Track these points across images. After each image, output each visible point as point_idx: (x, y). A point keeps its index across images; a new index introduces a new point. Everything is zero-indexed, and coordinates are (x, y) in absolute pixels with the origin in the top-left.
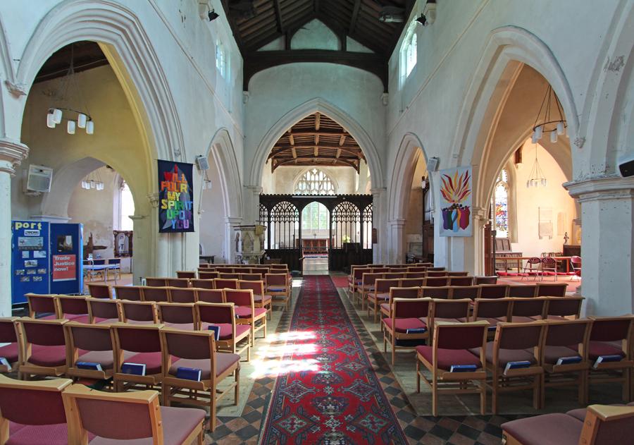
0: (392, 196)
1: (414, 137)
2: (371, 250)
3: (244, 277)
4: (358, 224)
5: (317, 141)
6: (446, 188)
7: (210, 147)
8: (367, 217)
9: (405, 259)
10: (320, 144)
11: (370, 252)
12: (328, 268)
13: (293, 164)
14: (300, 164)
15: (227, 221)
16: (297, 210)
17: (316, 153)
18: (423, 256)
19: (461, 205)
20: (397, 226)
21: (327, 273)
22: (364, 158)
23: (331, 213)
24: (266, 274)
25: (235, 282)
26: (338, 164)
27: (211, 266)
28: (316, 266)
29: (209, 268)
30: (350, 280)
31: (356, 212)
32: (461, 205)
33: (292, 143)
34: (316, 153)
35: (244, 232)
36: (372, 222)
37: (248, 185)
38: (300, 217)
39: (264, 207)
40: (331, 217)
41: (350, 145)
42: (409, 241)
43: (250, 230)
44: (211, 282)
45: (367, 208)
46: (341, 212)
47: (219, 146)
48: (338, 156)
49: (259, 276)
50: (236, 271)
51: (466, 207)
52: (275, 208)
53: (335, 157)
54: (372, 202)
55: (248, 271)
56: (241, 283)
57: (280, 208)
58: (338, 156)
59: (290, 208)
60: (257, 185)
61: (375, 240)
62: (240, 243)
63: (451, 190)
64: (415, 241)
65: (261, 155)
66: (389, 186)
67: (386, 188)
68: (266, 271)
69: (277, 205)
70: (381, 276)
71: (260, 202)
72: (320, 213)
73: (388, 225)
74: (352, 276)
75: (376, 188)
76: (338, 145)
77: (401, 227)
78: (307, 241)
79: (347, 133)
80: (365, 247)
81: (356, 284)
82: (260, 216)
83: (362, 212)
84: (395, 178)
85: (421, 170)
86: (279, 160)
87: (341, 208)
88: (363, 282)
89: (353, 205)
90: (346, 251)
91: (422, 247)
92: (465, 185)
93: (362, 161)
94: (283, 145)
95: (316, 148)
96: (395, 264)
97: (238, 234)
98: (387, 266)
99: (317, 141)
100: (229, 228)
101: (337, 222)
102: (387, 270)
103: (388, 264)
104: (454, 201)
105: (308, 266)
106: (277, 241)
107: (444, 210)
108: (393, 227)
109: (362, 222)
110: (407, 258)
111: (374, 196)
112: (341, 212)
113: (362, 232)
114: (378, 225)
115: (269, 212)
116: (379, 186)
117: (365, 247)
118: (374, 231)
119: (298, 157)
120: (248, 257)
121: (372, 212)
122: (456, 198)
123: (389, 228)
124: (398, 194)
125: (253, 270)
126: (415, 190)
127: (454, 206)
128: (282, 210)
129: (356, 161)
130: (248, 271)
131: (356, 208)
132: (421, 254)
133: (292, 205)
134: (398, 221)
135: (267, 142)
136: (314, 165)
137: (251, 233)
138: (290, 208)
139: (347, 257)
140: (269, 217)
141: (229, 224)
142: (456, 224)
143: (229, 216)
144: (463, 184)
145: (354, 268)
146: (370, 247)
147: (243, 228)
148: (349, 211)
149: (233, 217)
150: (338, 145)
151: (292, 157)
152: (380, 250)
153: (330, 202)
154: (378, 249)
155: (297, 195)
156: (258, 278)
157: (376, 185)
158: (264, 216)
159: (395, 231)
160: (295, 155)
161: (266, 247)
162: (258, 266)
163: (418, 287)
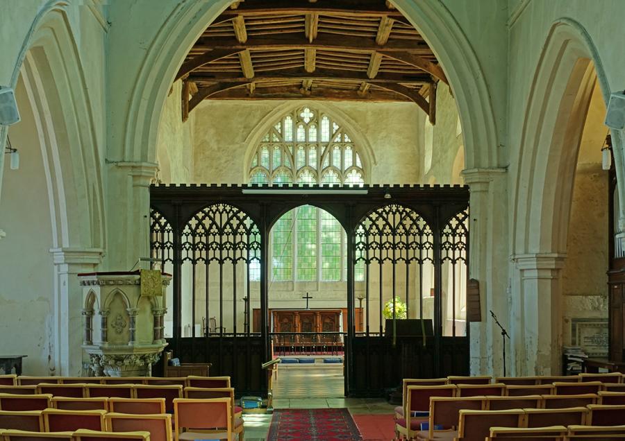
0: (523, 191)
1: (578, 32)
2: (465, 341)
3: (117, 407)
4: (428, 268)
5: (312, 31)
7: (18, 64)
9: (559, 363)
10: (321, 39)
11: (461, 345)
12: (342, 391)
13: (245, 95)
14: (262, 93)
15: (60, 258)
16: (255, 229)
17: (310, 67)
18: (610, 356)
20: (535, 274)
23: (351, 235)
24: (176, 400)
25: (98, 417)
26: (372, 95)
27: (24, 382)
28: (308, 383)
29: (15, 386)
30: (399, 416)
31: (421, 233)
33: (242, 36)
34: (310, 67)
35: (110, 290)
36: (467, 262)
37: (117, 158)
38: (263, 246)
39: (163, 221)
40: (352, 247)
41: (408, 44)
42: (570, 315)
43: (125, 284)
44: (37, 417)
45: (454, 222)
46: (381, 233)
47: (39, 52)
48: (372, 74)
49: (159, 404)
50: (94, 392)
52: (193, 222)
53: (363, 75)
54: (467, 205)
55: (125, 393)
56: (114, 420)
57: (207, 222)
58: (372, 74)
59: (235, 222)
60: (144, 157)
61: (474, 313)
62: (97, 320)
64: (587, 315)
65: (154, 73)
67: (506, 168)
68: (175, 393)
69: (200, 215)
70: (478, 404)
71: (152, 206)
72: (323, 235)
73: (513, 271)
74: (404, 410)
75: (477, 166)
76: (372, 42)
77: (549, 274)
79: (395, 10)
80: (447, 333)
81: (415, 428)
82: (152, 245)
83: (437, 233)
84: (530, 143)
85: (596, 126)
86: (202, 82)
87: (381, 223)
88: (430, 420)
89: (415, 215)
91: (606, 331)
93: (442, 87)
94: (216, 43)
95: (311, 52)
96: (532, 375)
97: (92, 295)
98: (500, 381)
99: (312, 31)
100: (65, 278)
102: (497, 391)
103: (501, 377)
105: (286, 385)
106: (201, 314)
108: (526, 274)
109: (438, 262)
110: (565, 361)
111: (471, 190)
112: (381, 233)
114: (483, 269)
115: (178, 233)
116: (485, 162)
117: (447, 333)
118: (473, 286)
119: (258, 75)
120: (119, 359)
121: (467, 234)
123: (516, 280)
124: (539, 186)
125: (139, 390)
126: (585, 172)
128: (214, 229)
129: (426, 85)
130: (125, 393)
131: (422, 223)
132: (605, 351)
133: (242, 215)
134: (538, 258)
135: (173, 38)
136: (304, 97)
137: (129, 292)
138: (235, 222)
139: (394, 360)
140: (177, 247)
141: (65, 268)
143: (66, 245)
145: (410, 386)
146: (461, 333)
147: (105, 278)
148: (401, 230)
149: (78, 247)
150: (372, 42)
151: (242, 75)
153: (350, 207)
154: (483, 339)
155: (255, 187)
156: (156, 408)
157: (477, 157)
158: (163, 246)
159: (532, 288)
160: (249, 72)
161: (168, 332)
162: (150, 382)
163: (562, 427)
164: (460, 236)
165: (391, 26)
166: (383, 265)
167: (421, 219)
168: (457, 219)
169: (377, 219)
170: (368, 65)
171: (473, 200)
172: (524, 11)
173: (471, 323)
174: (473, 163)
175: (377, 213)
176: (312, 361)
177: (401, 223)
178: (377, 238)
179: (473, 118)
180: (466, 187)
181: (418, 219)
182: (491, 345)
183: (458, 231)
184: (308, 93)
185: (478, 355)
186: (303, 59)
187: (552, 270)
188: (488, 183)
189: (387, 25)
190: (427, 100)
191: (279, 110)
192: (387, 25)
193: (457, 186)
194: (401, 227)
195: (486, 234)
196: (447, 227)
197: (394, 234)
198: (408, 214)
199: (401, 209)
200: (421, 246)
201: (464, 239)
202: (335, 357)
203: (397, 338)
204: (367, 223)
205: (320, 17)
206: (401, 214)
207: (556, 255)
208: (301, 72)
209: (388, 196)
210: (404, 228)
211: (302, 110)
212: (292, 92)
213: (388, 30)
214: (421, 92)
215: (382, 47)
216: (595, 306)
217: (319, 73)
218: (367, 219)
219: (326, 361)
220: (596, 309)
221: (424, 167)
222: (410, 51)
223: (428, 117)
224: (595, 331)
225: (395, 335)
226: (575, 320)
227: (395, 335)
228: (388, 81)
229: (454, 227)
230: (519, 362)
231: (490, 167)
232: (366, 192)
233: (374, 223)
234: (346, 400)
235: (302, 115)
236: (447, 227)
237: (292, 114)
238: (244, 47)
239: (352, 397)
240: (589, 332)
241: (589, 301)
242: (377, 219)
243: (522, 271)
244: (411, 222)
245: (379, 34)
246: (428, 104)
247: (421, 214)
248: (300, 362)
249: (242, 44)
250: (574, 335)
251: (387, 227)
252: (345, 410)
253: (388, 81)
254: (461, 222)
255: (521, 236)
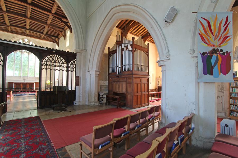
2: (75, 91)
4: (65, 73)
6: (205, 31)
8: (72, 68)
11: (73, 93)
12: (36, 106)
13: (7, 31)
14: (12, 32)
19: (221, 51)
20: (94, 75)
21: (35, 114)
22: (70, 28)
23: (41, 61)
26: (44, 39)
28: (24, 103)
31: (63, 63)
32: (221, 51)
34: (28, 27)
36: (75, 72)
40: (41, 65)
42: (100, 85)
45: (72, 62)
48: (45, 33)
51: (227, 52)
53: (42, 33)
58: (45, 33)
61: (77, 84)
63: (211, 35)
64: (103, 85)
66: (89, 49)
67: (86, 50)
72: (30, 67)
73: (88, 74)
76: (46, 23)
77: (97, 75)
78: (10, 84)
80: (70, 89)
83: (68, 64)
87: (51, 59)
89: (61, 58)
90: (57, 93)
92: (225, 30)
101: (46, 69)
104: (214, 46)
105: (16, 104)
107: (204, 54)
108: (91, 75)
109: (67, 71)
111: (77, 54)
113: (60, 77)
116: (81, 48)
117: (70, 89)
118: (77, 78)
121: (76, 65)
122: (216, 43)
127: (214, 51)
131: (63, 61)
134: (96, 71)
136: (26, 36)
142: (216, 69)
144: (223, 29)
146: (73, 89)
148: (57, 62)
152: (81, 91)
153: (41, 53)
160: (8, 24)
164: (74, 65)
165: (51, 20)
166: (51, 71)
167: (63, 60)
168: (73, 61)
169: (50, 58)
170: (44, 30)
171: (77, 57)
172: (102, 5)
173: (76, 87)
174: (78, 48)
175: (50, 56)
176: (26, 95)
177: (57, 60)
178: (50, 63)
179: (78, 36)
180: (76, 53)
181: (62, 59)
182: (82, 92)
183: (73, 64)
184: (27, 35)
185: (78, 94)
186: (26, 24)
187: (98, 74)
188: (81, 53)
189: (50, 19)
190: (57, 42)
191: (18, 37)
192: (50, 19)
193: (73, 53)
194: (57, 61)
195: (81, 65)
196: (70, 62)
197: (55, 63)
198: (59, 58)
199: (58, 56)
200: (63, 67)
201: (75, 66)
202: (32, 93)
203: (58, 92)
204: (47, 58)
205: (31, 8)
206: (57, 57)
207: (99, 71)
208: (25, 28)
209: (54, 52)
210: (58, 61)
211: (25, 39)
212: (22, 34)
213: (50, 21)
214: (56, 40)
215: (48, 25)
216: (105, 83)
217: (30, 29)
218: (47, 57)
219: (30, 95)
220: (104, 83)
221: (66, 45)
222: (55, 28)
223: (57, 45)
224: (105, 88)
225: (57, 91)
226: (101, 86)
227: (57, 91)
228: (48, 36)
229: (72, 63)
230: (89, 96)
231: (82, 49)
232: (47, 49)
233: (49, 59)
234: (38, 111)
235: (25, 40)
236: (70, 62)
237: (22, 39)
238: (5, 13)
239: (40, 109)
240: (103, 88)
241: (103, 82)
242: (50, 58)
243: (91, 74)
244: (61, 60)
245: (48, 21)
246: (57, 43)
247: (63, 58)
248: (22, 95)
249: (4, 12)
250: (100, 89)
251: (53, 60)
252: (38, 118)
253: (48, 36)
254: (74, 62)
255: (91, 66)
